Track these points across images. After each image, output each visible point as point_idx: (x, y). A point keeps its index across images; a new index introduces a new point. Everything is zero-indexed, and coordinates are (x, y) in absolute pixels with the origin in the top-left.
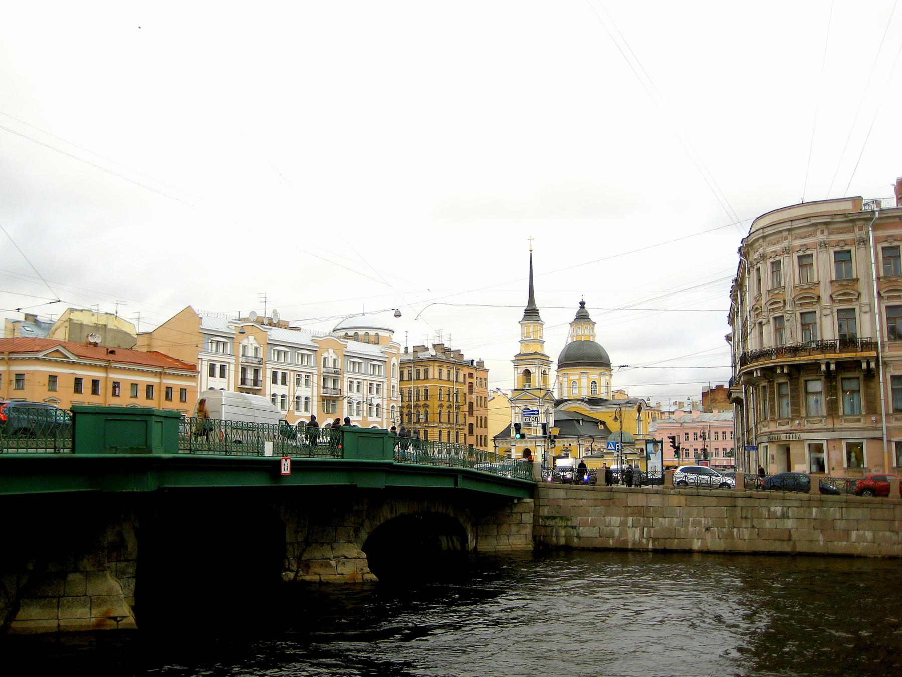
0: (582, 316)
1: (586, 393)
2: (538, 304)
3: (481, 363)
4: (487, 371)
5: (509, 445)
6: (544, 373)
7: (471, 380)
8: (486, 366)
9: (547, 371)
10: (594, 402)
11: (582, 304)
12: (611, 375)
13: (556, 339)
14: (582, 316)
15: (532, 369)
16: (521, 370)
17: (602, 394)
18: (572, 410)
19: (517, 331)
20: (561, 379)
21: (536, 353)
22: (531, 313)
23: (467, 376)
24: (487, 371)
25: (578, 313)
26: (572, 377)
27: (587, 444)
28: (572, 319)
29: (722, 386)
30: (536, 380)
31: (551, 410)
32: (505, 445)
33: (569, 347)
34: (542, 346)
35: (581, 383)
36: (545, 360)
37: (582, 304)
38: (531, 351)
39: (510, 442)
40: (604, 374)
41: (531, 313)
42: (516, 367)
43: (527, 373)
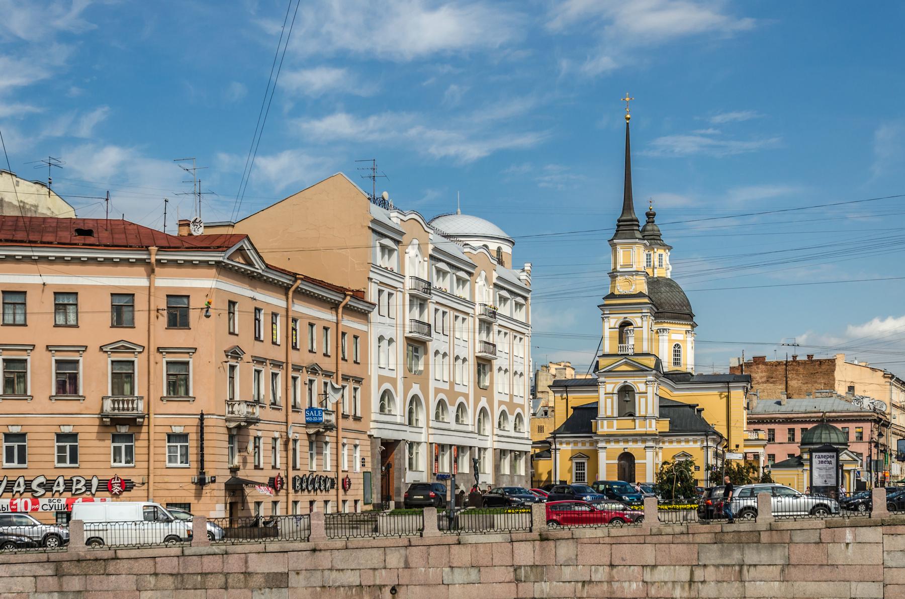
10: (680, 378)
15: (636, 319)
21: (640, 295)
29: (764, 358)
39: (597, 442)
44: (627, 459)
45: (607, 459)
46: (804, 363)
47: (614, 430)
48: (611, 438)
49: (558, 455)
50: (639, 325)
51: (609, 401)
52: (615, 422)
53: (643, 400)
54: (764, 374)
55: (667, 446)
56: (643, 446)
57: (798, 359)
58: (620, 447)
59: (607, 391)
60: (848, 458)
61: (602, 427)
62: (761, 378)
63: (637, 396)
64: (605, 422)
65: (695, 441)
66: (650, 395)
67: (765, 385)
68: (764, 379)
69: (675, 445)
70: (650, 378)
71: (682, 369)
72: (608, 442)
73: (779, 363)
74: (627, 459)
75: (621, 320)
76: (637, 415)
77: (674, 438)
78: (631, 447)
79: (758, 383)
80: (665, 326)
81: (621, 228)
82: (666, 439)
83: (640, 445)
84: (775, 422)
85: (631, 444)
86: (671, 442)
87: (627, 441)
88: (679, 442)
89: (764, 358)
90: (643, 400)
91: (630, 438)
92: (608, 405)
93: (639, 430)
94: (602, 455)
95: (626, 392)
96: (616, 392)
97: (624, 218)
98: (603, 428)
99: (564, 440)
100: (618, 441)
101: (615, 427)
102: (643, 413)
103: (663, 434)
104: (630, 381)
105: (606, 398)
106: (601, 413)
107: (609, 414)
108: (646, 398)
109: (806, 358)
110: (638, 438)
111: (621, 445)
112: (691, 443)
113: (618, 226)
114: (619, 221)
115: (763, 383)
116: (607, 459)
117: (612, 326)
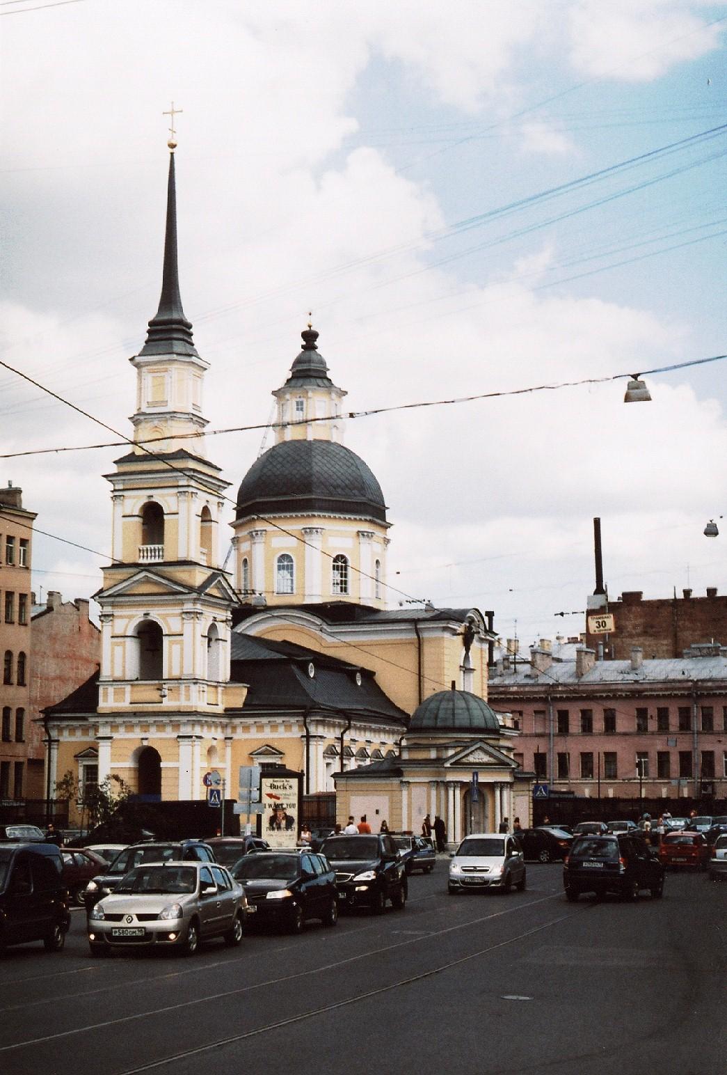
0: (308, 372)
1: (320, 589)
2: (190, 309)
4: (32, 516)
5: (89, 738)
6: (205, 514)
9: (213, 509)
10: (340, 614)
11: (310, 338)
12: (387, 541)
13: (236, 421)
14: (308, 372)
15: (167, 500)
16: (134, 503)
17: (360, 593)
18: (278, 637)
20: (245, 546)
21: (182, 454)
22: (169, 332)
24: (32, 516)
25: (298, 361)
27: (331, 734)
28: (280, 383)
29: (639, 594)
30: (182, 537)
31: (224, 632)
32: (79, 737)
33: (271, 457)
35: (303, 561)
37: (310, 338)
39: (95, 727)
40: (369, 535)
41: (169, 332)
42: (117, 496)
44: (148, 762)
45: (112, 761)
46: (700, 601)
47: (124, 705)
48: (119, 720)
49: (55, 753)
50: (174, 510)
52: (128, 688)
53: (176, 648)
54: (640, 621)
55: (240, 735)
56: (175, 735)
57: (694, 595)
58: (133, 737)
59: (119, 632)
60: (486, 759)
61: (106, 700)
62: (635, 627)
63: (166, 640)
64: (111, 690)
65: (288, 727)
66: (187, 638)
67: (641, 639)
68: (639, 630)
69: (254, 734)
70: (188, 607)
71: (351, 597)
72: (115, 727)
73: (662, 603)
74: (148, 762)
75: (146, 500)
76: (165, 676)
77: (250, 721)
78: (156, 737)
79: (631, 636)
80: (315, 523)
82: (237, 721)
83: (170, 733)
84: (615, 698)
85: (153, 729)
86: (246, 728)
87: (146, 727)
88: (261, 727)
89: (638, 595)
90: (176, 648)
91: (151, 720)
92: (118, 657)
93: (168, 704)
94: (104, 750)
96: (130, 632)
98: (108, 700)
99: (65, 723)
100: (130, 727)
101: (128, 698)
102: (176, 673)
103: (231, 713)
104: (156, 615)
105: (114, 644)
106: (106, 673)
107: (118, 674)
108: (181, 643)
109: (705, 595)
110: (165, 719)
111: (137, 734)
112: (253, 730)
113: (149, 332)
114: (151, 324)
115: (639, 635)
116: (112, 761)
117: (128, 513)
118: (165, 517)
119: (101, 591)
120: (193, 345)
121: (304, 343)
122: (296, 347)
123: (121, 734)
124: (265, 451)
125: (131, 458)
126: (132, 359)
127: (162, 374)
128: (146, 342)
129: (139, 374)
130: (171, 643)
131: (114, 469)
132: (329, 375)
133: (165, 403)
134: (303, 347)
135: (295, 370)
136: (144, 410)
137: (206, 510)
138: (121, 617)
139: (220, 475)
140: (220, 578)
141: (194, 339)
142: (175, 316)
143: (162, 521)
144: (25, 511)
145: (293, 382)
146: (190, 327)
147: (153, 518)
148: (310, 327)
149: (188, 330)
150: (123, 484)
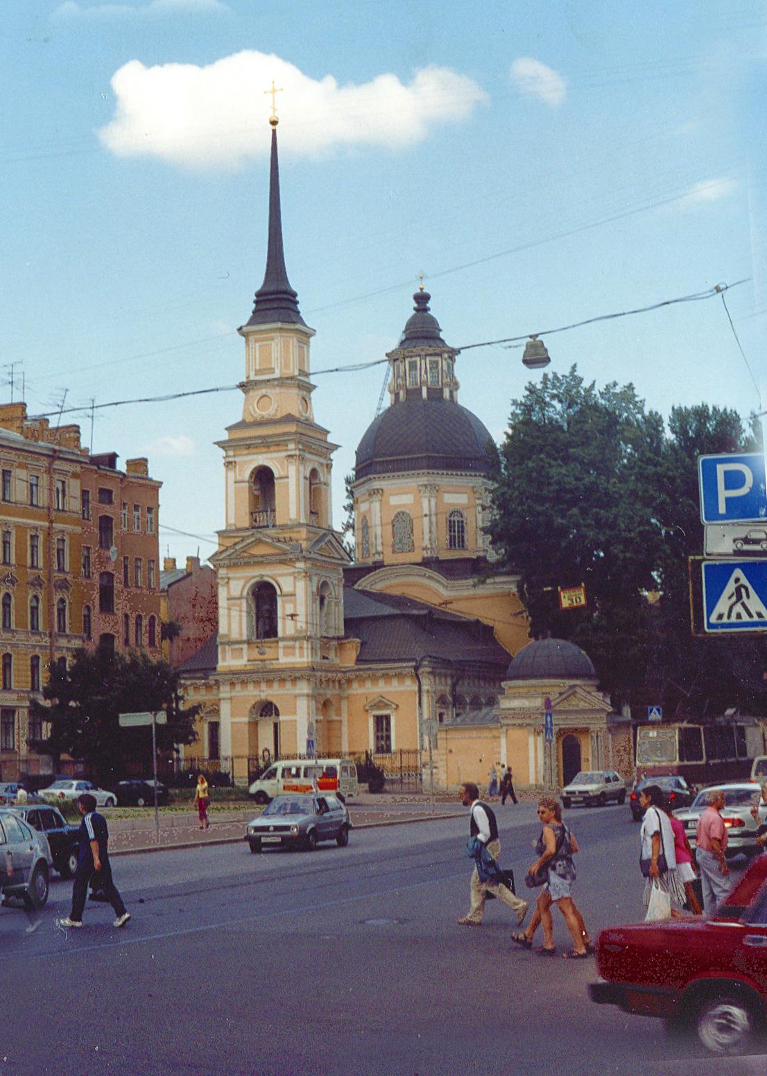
0: (422, 333)
3: (139, 465)
7: (107, 510)
8: (154, 473)
11: (422, 299)
14: (422, 333)
19: (235, 360)
21: (289, 419)
22: (276, 302)
23: (93, 496)
25: (411, 325)
26: (394, 501)
30: (290, 500)
34: (306, 401)
36: (314, 443)
37: (422, 299)
38: (270, 411)
41: (276, 302)
43: (264, 479)
50: (283, 474)
51: (235, 613)
61: (224, 659)
63: (279, 600)
76: (280, 634)
81: (260, 307)
92: (234, 620)
94: (225, 708)
95: (264, 596)
96: (245, 593)
97: (267, 289)
98: (228, 661)
113: (256, 302)
114: (258, 295)
117: (239, 478)
118: (276, 481)
119: (216, 554)
120: (299, 312)
121: (416, 305)
122: (408, 309)
123: (239, 691)
124: (381, 411)
125: (241, 425)
126: (240, 329)
127: (268, 342)
128: (254, 312)
129: (247, 342)
130: (283, 601)
131: (225, 436)
132: (442, 335)
133: (272, 370)
134: (415, 309)
135: (407, 332)
136: (252, 378)
137: (314, 473)
138: (235, 578)
139: (330, 439)
140: (330, 537)
141: (299, 307)
142: (282, 288)
143: (273, 484)
144: (151, 480)
145: (407, 342)
146: (295, 295)
147: (264, 479)
148: (421, 289)
149: (291, 298)
150: (234, 450)
